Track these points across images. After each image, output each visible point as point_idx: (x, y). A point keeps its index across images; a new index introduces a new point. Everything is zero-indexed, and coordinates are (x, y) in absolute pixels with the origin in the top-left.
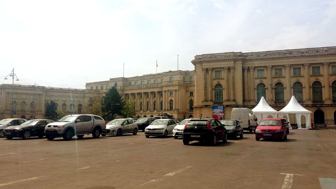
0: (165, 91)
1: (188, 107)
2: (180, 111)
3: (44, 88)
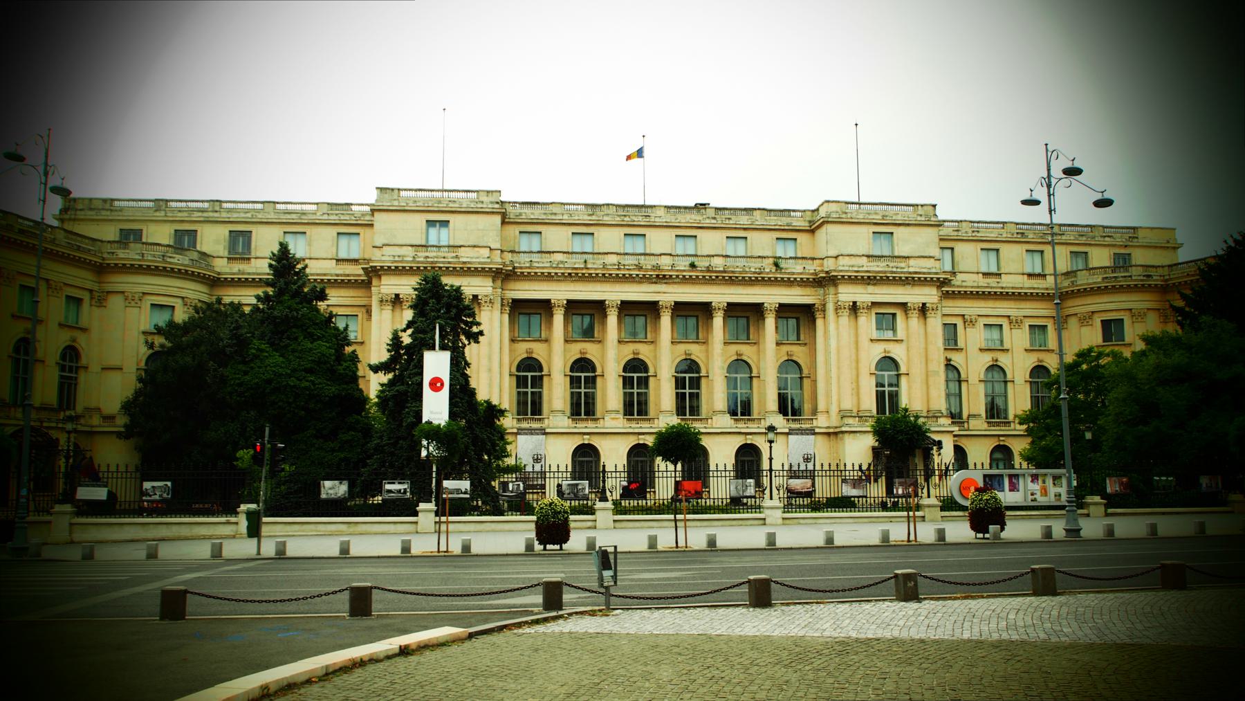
0: (854, 308)
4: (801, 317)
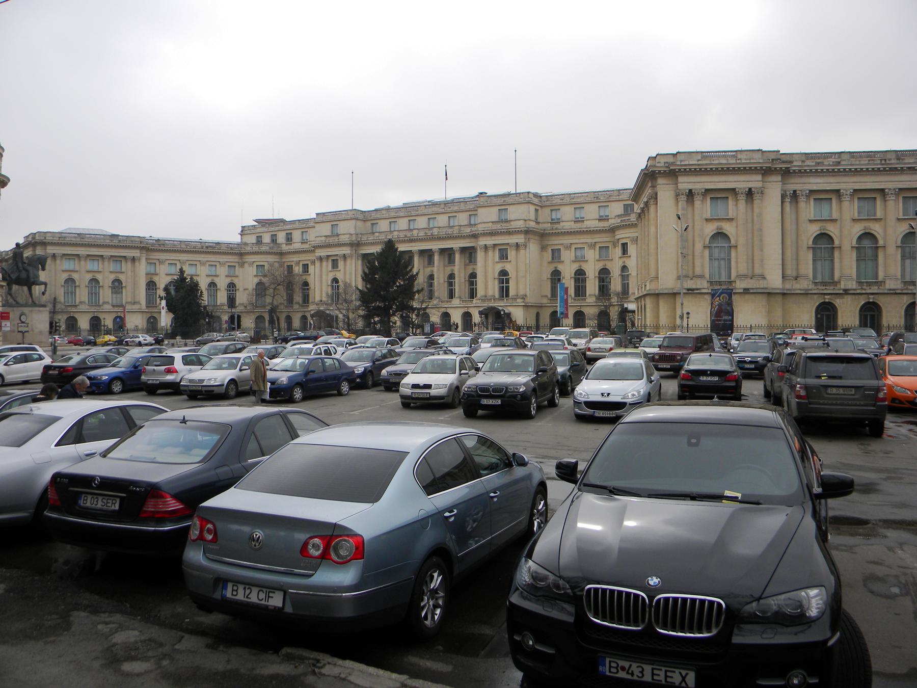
0: (486, 247)
1: (548, 291)
2: (530, 300)
3: (141, 240)
4: (469, 253)
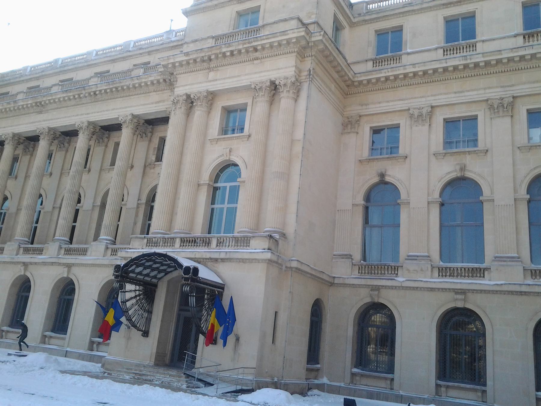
0: (190, 102)
2: (297, 254)
